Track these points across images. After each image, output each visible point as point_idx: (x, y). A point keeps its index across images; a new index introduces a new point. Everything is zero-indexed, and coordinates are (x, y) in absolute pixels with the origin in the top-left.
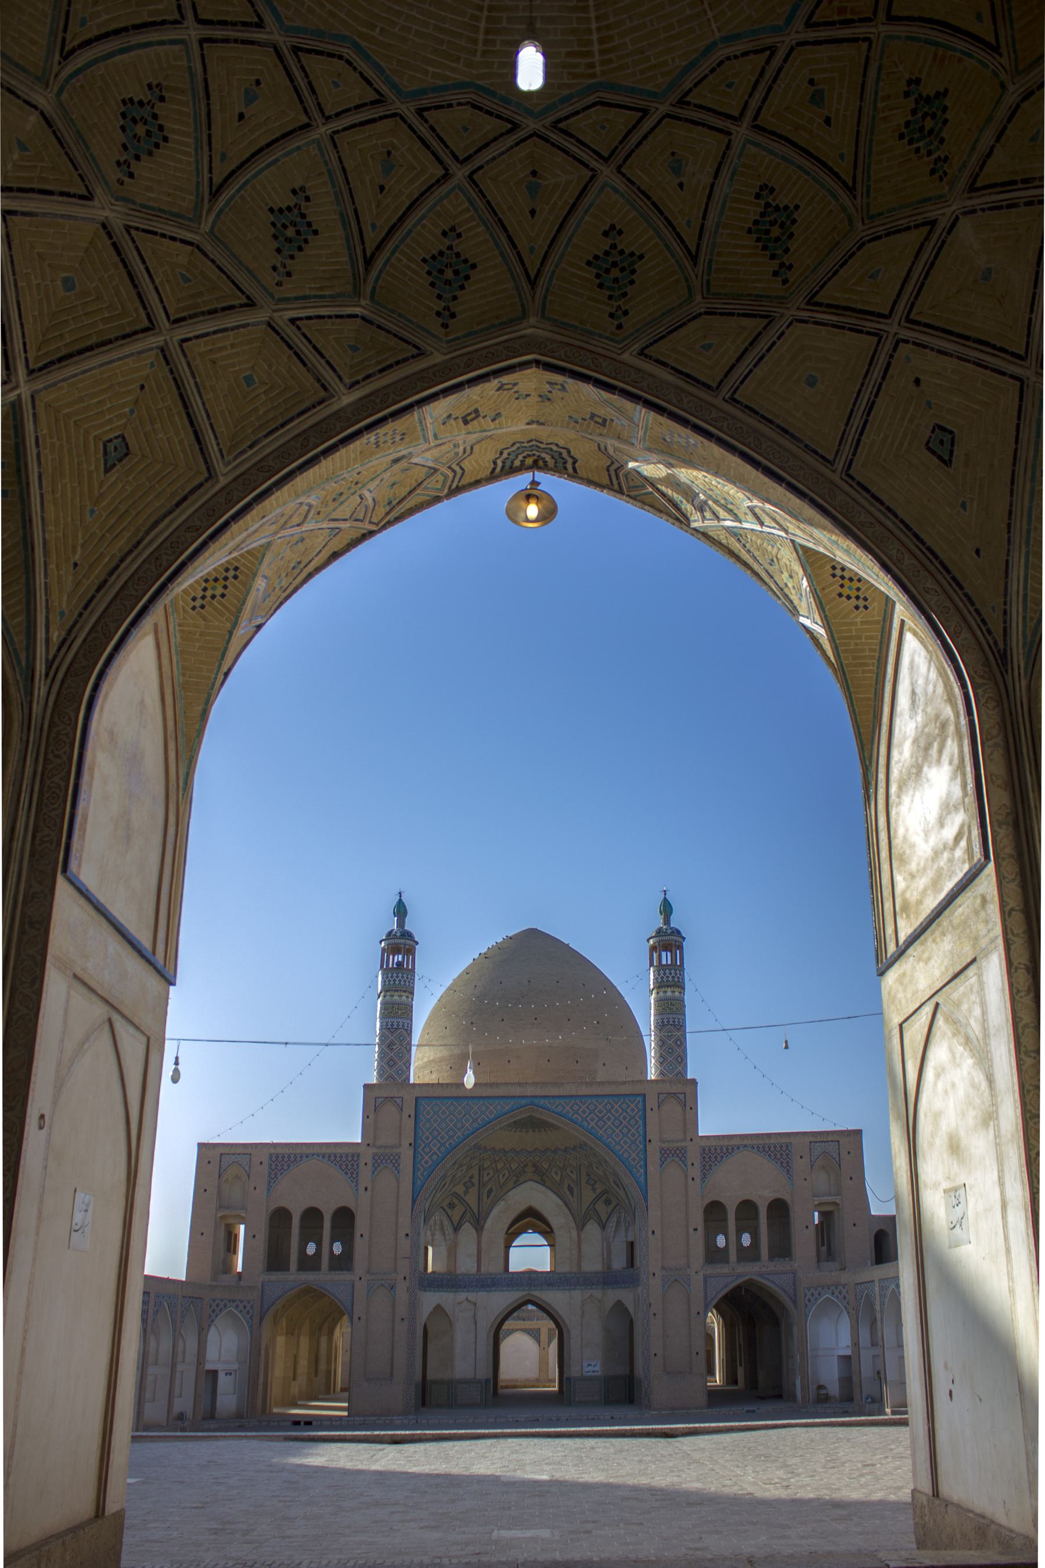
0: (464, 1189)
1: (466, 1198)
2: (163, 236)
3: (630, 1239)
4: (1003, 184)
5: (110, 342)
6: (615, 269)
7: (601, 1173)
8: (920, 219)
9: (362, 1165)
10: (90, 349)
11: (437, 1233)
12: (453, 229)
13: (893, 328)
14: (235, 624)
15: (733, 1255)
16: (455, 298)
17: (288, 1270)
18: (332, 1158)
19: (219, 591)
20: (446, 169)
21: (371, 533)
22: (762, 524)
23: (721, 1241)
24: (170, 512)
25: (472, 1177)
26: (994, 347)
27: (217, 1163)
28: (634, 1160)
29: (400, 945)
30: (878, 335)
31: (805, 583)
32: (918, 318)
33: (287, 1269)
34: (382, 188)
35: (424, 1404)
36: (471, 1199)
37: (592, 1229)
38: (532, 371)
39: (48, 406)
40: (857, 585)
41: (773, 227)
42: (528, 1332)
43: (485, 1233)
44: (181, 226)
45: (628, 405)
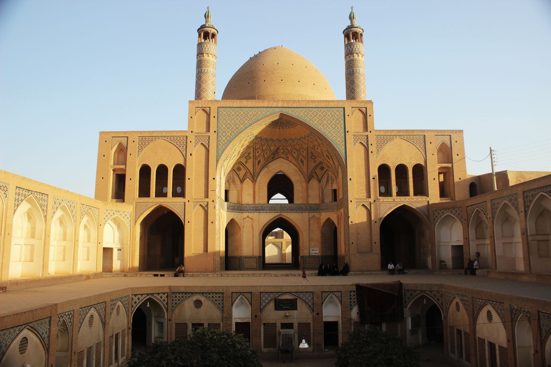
0: (245, 160)
1: (246, 165)
3: (335, 187)
7: (319, 151)
9: (188, 142)
11: (231, 183)
17: (149, 196)
18: (172, 139)
25: (249, 154)
28: (339, 141)
36: (250, 165)
37: (314, 183)
43: (257, 183)
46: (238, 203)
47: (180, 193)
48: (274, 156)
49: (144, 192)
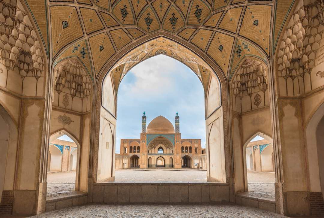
2: (105, 13)
4: (236, 3)
5: (98, 30)
6: (173, 20)
8: (222, 10)
10: (96, 31)
12: (149, 13)
13: (216, 30)
14: (121, 75)
15: (185, 152)
16: (150, 25)
19: (119, 70)
20: (148, 3)
21: (139, 63)
22: (193, 61)
23: (183, 151)
24: (111, 58)
26: (231, 32)
27: (123, 142)
29: (144, 118)
30: (213, 31)
31: (199, 70)
32: (220, 28)
33: (132, 153)
34: (138, 6)
35: (149, 167)
37: (168, 149)
38: (162, 38)
39: (91, 40)
40: (206, 70)
41: (198, 13)
42: (160, 160)
44: (107, 11)
45: (175, 43)
46: (151, 153)
47: (139, 152)
48: (159, 143)
49: (131, 152)
